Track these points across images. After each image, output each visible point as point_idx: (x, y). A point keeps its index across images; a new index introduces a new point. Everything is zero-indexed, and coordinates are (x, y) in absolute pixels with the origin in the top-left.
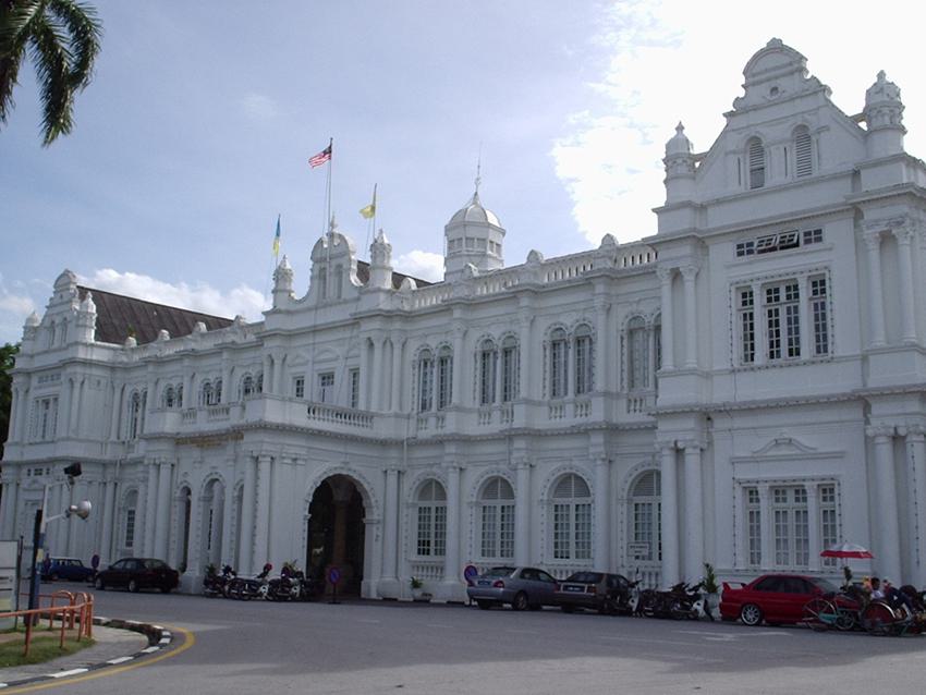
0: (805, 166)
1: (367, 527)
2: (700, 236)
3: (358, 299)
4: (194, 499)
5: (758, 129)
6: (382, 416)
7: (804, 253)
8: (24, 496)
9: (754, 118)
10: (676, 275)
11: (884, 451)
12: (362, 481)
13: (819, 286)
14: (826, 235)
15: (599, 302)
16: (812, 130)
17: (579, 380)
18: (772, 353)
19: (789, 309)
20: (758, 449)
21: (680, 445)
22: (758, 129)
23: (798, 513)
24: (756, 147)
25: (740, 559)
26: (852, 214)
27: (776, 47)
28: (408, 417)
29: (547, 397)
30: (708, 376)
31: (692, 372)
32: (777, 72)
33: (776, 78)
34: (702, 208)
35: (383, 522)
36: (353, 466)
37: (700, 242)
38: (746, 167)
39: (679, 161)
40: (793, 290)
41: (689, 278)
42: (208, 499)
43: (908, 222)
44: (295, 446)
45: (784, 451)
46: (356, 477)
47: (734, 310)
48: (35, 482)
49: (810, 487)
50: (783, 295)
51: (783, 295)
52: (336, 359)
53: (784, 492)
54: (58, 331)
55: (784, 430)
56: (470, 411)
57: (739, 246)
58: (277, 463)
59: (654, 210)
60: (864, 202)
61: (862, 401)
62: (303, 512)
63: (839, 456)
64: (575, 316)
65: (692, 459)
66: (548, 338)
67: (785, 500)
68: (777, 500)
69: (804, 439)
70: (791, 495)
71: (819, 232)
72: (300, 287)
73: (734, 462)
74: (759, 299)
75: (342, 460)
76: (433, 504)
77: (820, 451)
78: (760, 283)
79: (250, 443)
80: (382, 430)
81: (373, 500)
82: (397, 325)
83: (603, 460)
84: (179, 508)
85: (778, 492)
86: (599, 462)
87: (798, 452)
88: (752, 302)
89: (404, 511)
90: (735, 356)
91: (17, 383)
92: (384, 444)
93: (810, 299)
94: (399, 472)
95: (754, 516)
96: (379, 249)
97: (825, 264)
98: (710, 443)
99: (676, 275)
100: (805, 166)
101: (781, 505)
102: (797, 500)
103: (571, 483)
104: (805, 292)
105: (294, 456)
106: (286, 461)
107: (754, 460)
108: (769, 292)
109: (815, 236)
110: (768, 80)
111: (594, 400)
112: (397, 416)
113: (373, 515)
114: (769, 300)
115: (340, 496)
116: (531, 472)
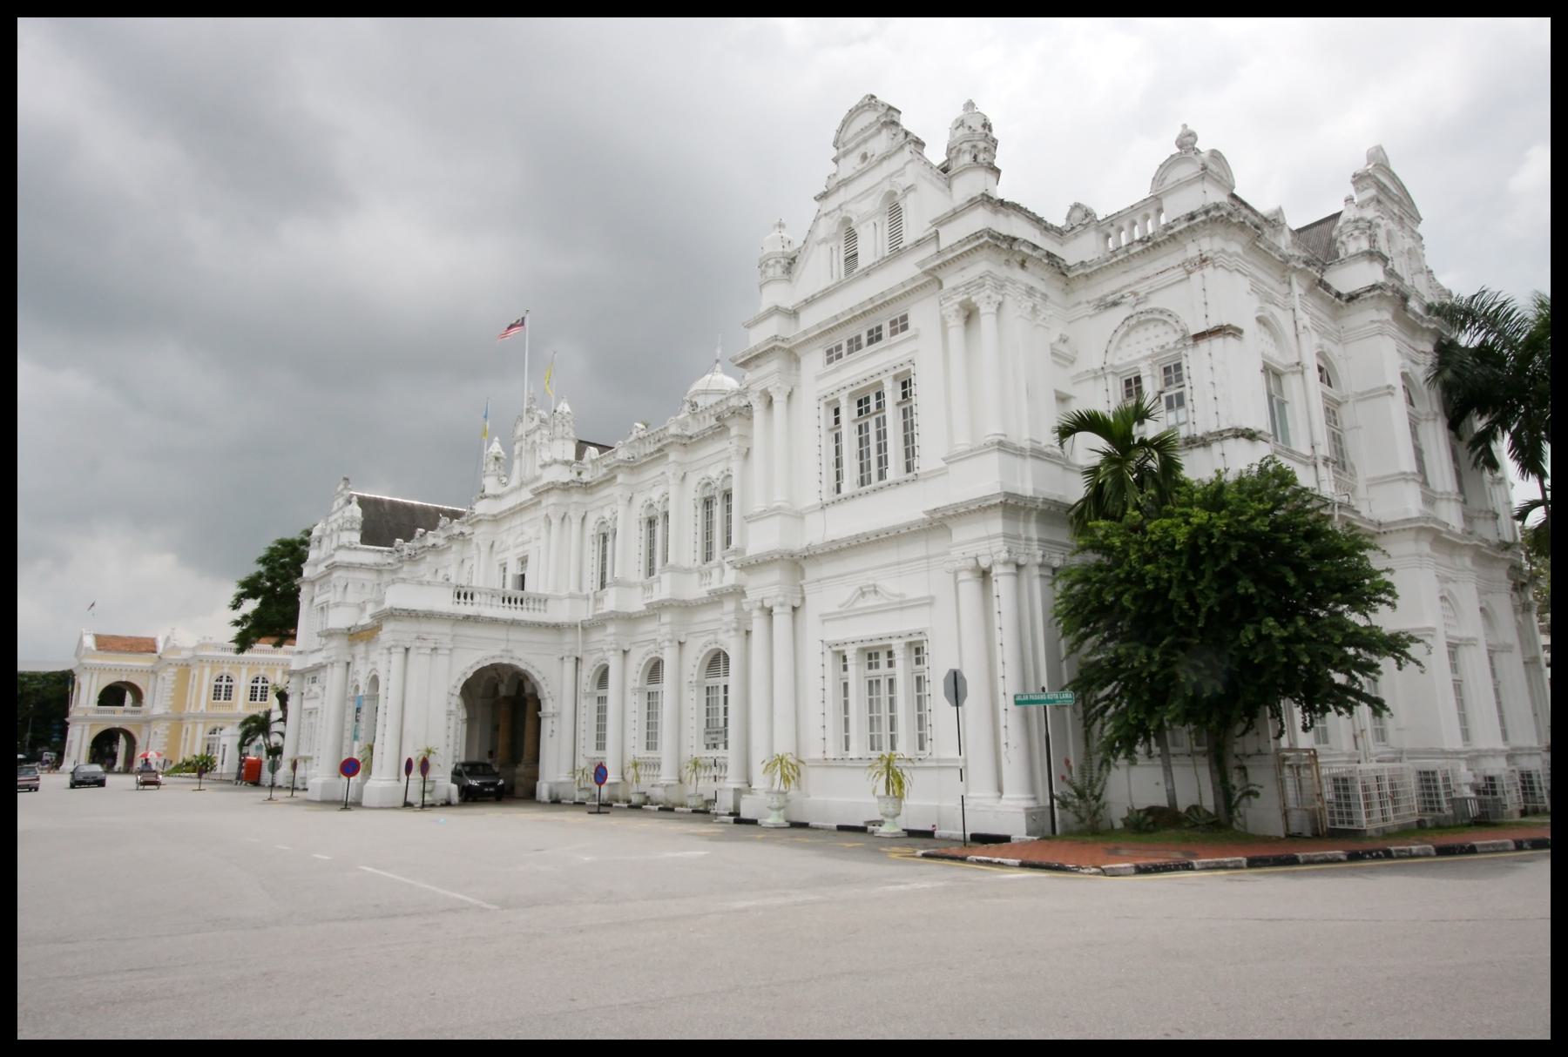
1: (543, 722)
2: (787, 346)
6: (560, 599)
7: (890, 347)
11: (970, 588)
16: (899, 192)
19: (878, 420)
21: (767, 604)
23: (891, 681)
25: (830, 744)
26: (936, 286)
28: (587, 598)
29: (699, 562)
30: (800, 516)
31: (777, 511)
33: (865, 141)
34: (794, 314)
36: (519, 653)
39: (771, 262)
43: (989, 282)
44: (440, 631)
45: (871, 601)
46: (522, 666)
47: (823, 431)
49: (898, 647)
53: (877, 655)
54: (335, 537)
56: (631, 586)
57: (829, 352)
60: (939, 266)
61: (939, 523)
63: (929, 602)
64: (721, 466)
65: (781, 620)
66: (698, 496)
67: (877, 666)
69: (892, 585)
70: (883, 659)
71: (904, 318)
73: (826, 618)
74: (848, 413)
75: (503, 646)
78: (846, 392)
80: (559, 613)
81: (546, 690)
82: (576, 497)
85: (870, 656)
86: (732, 633)
87: (883, 601)
89: (583, 702)
90: (824, 488)
92: (557, 627)
93: (899, 404)
98: (803, 599)
101: (874, 672)
102: (890, 664)
103: (717, 661)
104: (892, 395)
109: (901, 325)
110: (858, 146)
112: (571, 596)
113: (548, 707)
114: (860, 413)
115: (528, 690)
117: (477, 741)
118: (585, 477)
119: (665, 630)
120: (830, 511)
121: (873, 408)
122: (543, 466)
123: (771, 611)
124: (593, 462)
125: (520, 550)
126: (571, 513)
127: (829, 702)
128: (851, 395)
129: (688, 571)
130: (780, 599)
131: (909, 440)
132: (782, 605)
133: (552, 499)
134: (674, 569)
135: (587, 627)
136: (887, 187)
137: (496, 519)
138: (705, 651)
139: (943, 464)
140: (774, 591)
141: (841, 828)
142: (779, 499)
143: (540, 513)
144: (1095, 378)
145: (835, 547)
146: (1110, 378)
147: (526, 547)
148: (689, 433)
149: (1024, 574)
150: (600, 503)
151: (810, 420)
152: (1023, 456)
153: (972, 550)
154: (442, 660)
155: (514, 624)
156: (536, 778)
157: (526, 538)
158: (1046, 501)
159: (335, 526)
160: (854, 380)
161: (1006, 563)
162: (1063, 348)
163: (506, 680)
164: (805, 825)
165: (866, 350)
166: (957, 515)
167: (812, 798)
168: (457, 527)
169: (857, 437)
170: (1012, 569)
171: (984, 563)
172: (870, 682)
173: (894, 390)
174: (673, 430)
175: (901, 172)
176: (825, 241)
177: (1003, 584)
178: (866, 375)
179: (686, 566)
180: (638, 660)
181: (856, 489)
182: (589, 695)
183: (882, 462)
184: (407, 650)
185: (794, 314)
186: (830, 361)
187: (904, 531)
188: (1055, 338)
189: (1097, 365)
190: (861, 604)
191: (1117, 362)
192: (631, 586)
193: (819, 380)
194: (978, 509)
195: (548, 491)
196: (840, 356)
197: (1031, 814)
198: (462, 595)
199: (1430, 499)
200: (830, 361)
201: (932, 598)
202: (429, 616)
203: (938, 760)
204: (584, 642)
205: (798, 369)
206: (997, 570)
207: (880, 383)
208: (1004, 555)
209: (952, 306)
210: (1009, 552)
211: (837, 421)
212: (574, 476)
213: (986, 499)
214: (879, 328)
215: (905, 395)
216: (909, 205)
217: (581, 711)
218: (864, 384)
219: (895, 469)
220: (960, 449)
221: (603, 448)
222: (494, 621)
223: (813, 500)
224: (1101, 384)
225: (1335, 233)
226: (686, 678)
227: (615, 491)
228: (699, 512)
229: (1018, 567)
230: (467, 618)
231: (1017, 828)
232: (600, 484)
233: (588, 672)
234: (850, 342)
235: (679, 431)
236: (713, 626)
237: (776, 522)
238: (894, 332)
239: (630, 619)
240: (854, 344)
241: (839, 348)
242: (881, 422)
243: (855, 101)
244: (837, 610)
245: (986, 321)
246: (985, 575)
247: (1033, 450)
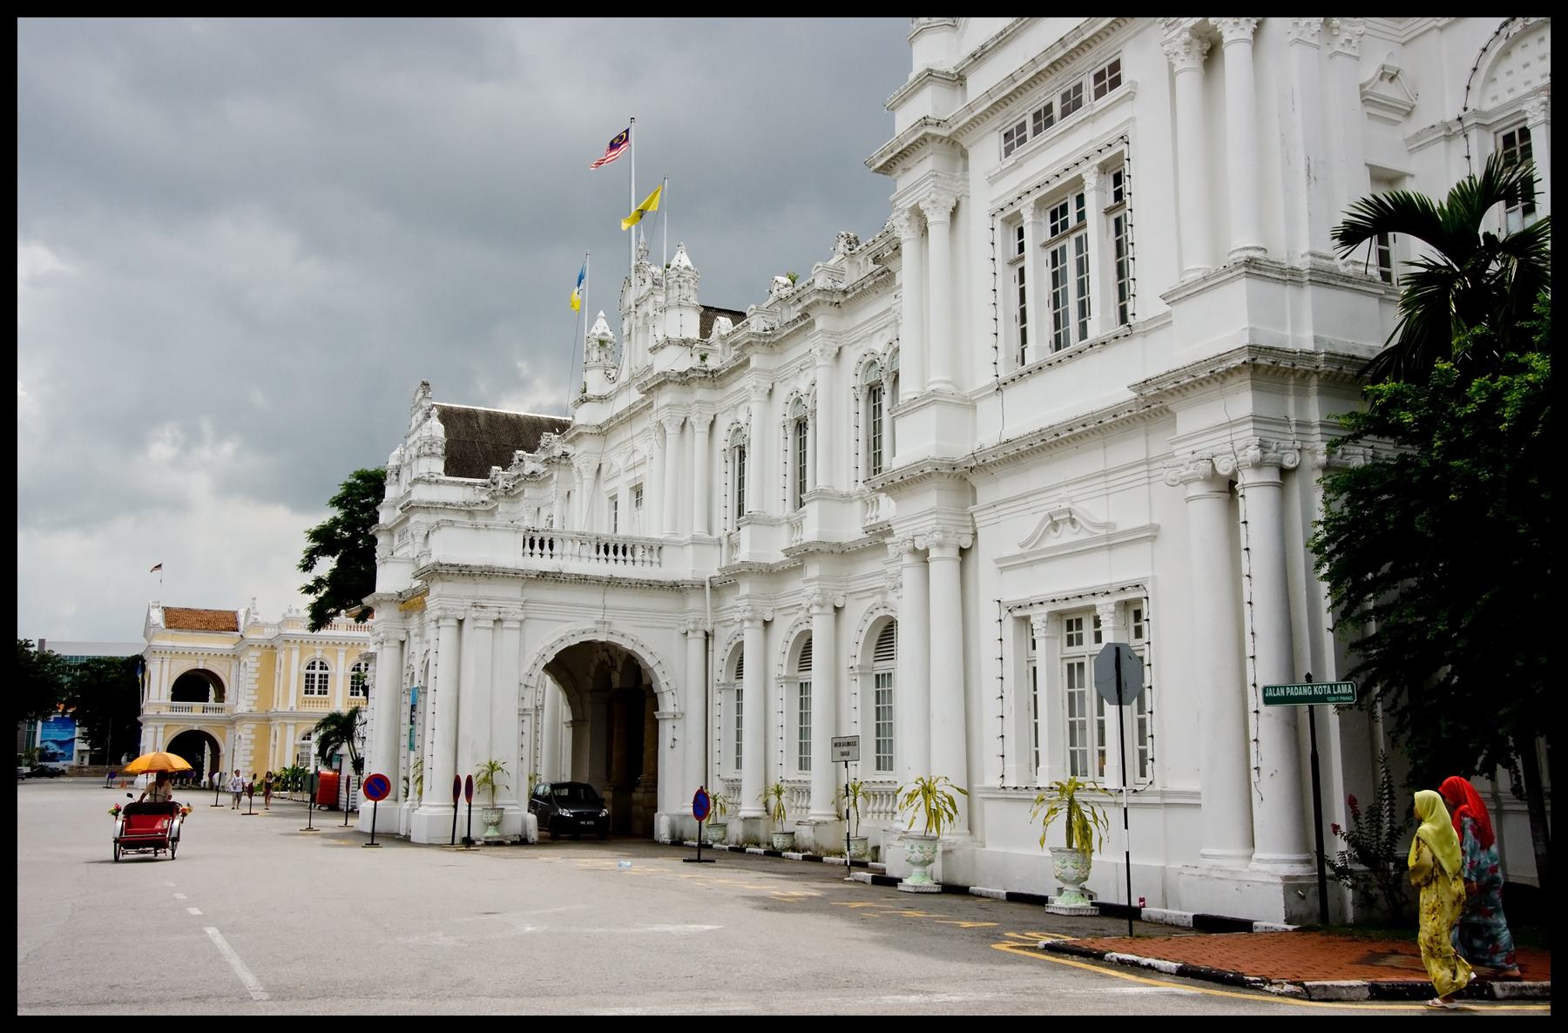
2: (944, 132)
6: (680, 545)
11: (1205, 511)
14: (1126, 73)
18: (1057, 337)
19: (1079, 240)
20: (1029, 534)
25: (1011, 765)
34: (958, 80)
44: (506, 596)
45: (1067, 536)
46: (627, 645)
47: (1000, 266)
49: (1105, 608)
53: (1079, 622)
55: (1063, 492)
56: (772, 523)
61: (1155, 403)
63: (1150, 535)
64: (889, 335)
66: (859, 382)
67: (1080, 642)
68: (1070, 643)
69: (1096, 509)
71: (1115, 66)
73: (1006, 565)
74: (1037, 231)
75: (599, 617)
77: (1122, 527)
80: (678, 567)
81: (662, 681)
82: (700, 393)
85: (1071, 623)
87: (1083, 536)
89: (716, 698)
90: (1002, 355)
93: (1108, 212)
94: (707, 634)
97: (1120, 132)
98: (975, 534)
101: (1075, 650)
105: (496, 616)
106: (480, 624)
112: (696, 542)
113: (667, 706)
114: (1054, 231)
115: (645, 681)
116: (837, 619)
117: (586, 757)
118: (713, 363)
119: (812, 588)
120: (1011, 393)
122: (653, 350)
123: (926, 552)
124: (722, 339)
125: (631, 476)
126: (693, 419)
127: (1010, 697)
128: (1039, 203)
129: (846, 498)
130: (938, 537)
132: (940, 545)
133: (665, 398)
134: (822, 495)
135: (720, 587)
137: (603, 431)
138: (872, 619)
139: (1163, 308)
140: (929, 523)
141: (1013, 897)
142: (937, 378)
143: (648, 421)
144: (1448, 138)
145: (1011, 451)
146: (1474, 135)
148: (843, 286)
149: (1296, 485)
150: (733, 401)
152: (1299, 284)
153: (1206, 446)
154: (509, 637)
155: (612, 583)
156: (654, 808)
157: (637, 458)
158: (1331, 357)
159: (414, 451)
160: (1040, 179)
161: (1258, 465)
162: (1387, 90)
163: (620, 664)
164: (962, 891)
165: (1060, 126)
166: (1181, 390)
167: (989, 848)
169: (1049, 271)
170: (1271, 475)
171: (1224, 467)
172: (1071, 666)
173: (1100, 189)
174: (819, 284)
177: (1256, 503)
178: (1058, 169)
179: (844, 490)
180: (783, 635)
181: (1051, 356)
182: (726, 687)
183: (1083, 309)
184: (461, 622)
185: (958, 80)
186: (1008, 152)
187: (1108, 420)
188: (1370, 72)
189: (1450, 115)
190: (1052, 541)
191: (1488, 106)
192: (772, 523)
194: (1212, 377)
195: (659, 386)
196: (1023, 140)
197: (1292, 886)
198: (537, 542)
200: (1008, 152)
201: (1157, 528)
202: (489, 574)
203: (1163, 794)
204: (715, 610)
205: (966, 168)
206: (1246, 478)
207: (1079, 181)
208: (1254, 453)
210: (1262, 446)
211: (1021, 248)
212: (695, 362)
213: (1220, 358)
214: (1078, 89)
215: (1118, 195)
217: (714, 711)
218: (1056, 184)
219: (1101, 321)
220: (1190, 277)
221: (737, 316)
222: (582, 580)
223: (986, 379)
224: (1459, 146)
226: (846, 661)
227: (747, 381)
228: (862, 404)
229: (1285, 473)
230: (543, 575)
232: (731, 371)
233: (720, 652)
234: (1037, 116)
235: (829, 284)
236: (879, 582)
237: (930, 415)
238: (1099, 93)
239: (770, 573)
240: (1044, 118)
241: (1022, 128)
242: (1081, 245)
244: (1019, 551)
247: (1314, 271)
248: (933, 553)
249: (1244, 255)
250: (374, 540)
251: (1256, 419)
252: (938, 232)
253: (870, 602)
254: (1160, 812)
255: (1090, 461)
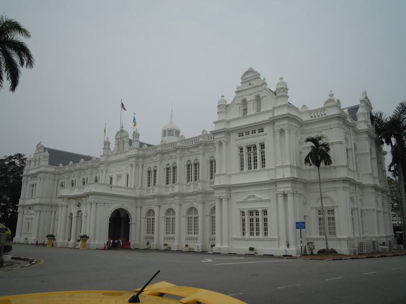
0: (259, 110)
3: (128, 151)
4: (73, 217)
5: (246, 97)
8: (25, 216)
9: (244, 93)
10: (220, 143)
11: (281, 199)
12: (128, 210)
13: (262, 146)
14: (265, 131)
15: (201, 152)
17: (196, 177)
19: (254, 154)
21: (221, 198)
22: (246, 97)
23: (257, 219)
24: (245, 102)
27: (250, 71)
30: (230, 176)
32: (250, 77)
34: (228, 122)
35: (135, 224)
37: (228, 132)
38: (242, 108)
40: (255, 147)
41: (224, 144)
42: (77, 217)
48: (29, 211)
50: (252, 149)
51: (252, 149)
52: (122, 170)
53: (253, 212)
54: (37, 162)
55: (252, 192)
57: (240, 134)
58: (98, 205)
59: (214, 122)
61: (275, 183)
62: (106, 221)
63: (269, 201)
65: (225, 203)
67: (253, 215)
68: (251, 215)
69: (258, 196)
70: (254, 214)
72: (113, 146)
73: (238, 203)
74: (245, 150)
76: (151, 217)
79: (91, 199)
83: (201, 203)
84: (68, 220)
85: (251, 213)
88: (256, 149)
91: (24, 179)
95: (244, 220)
96: (136, 135)
98: (231, 197)
99: (220, 143)
100: (259, 110)
102: (256, 215)
103: (192, 209)
107: (244, 202)
108: (248, 148)
111: (199, 184)
113: (133, 221)
114: (248, 151)
115: (122, 215)
121: (252, 151)
126: (139, 164)
131: (263, 159)
136: (257, 94)
147: (121, 172)
151: (235, 152)
153: (282, 190)
168: (90, 163)
170: (292, 195)
171: (286, 193)
175: (262, 91)
176: (238, 104)
182: (145, 218)
183: (255, 164)
193: (236, 142)
199: (374, 178)
200: (240, 136)
209: (277, 129)
216: (264, 101)
225: (357, 114)
231: (294, 254)
243: (247, 70)
245: (287, 135)
246: (285, 195)
248: (223, 200)
249: (289, 164)
250: (22, 178)
251: (291, 187)
252: (224, 147)
253: (189, 204)
254: (269, 242)
255: (259, 189)
